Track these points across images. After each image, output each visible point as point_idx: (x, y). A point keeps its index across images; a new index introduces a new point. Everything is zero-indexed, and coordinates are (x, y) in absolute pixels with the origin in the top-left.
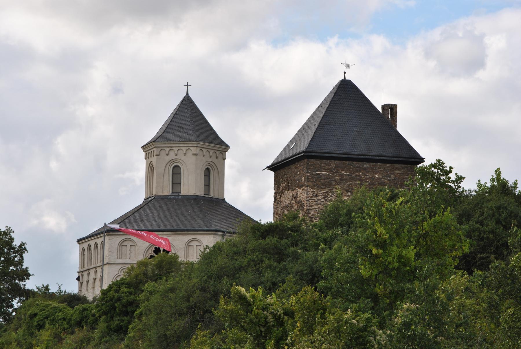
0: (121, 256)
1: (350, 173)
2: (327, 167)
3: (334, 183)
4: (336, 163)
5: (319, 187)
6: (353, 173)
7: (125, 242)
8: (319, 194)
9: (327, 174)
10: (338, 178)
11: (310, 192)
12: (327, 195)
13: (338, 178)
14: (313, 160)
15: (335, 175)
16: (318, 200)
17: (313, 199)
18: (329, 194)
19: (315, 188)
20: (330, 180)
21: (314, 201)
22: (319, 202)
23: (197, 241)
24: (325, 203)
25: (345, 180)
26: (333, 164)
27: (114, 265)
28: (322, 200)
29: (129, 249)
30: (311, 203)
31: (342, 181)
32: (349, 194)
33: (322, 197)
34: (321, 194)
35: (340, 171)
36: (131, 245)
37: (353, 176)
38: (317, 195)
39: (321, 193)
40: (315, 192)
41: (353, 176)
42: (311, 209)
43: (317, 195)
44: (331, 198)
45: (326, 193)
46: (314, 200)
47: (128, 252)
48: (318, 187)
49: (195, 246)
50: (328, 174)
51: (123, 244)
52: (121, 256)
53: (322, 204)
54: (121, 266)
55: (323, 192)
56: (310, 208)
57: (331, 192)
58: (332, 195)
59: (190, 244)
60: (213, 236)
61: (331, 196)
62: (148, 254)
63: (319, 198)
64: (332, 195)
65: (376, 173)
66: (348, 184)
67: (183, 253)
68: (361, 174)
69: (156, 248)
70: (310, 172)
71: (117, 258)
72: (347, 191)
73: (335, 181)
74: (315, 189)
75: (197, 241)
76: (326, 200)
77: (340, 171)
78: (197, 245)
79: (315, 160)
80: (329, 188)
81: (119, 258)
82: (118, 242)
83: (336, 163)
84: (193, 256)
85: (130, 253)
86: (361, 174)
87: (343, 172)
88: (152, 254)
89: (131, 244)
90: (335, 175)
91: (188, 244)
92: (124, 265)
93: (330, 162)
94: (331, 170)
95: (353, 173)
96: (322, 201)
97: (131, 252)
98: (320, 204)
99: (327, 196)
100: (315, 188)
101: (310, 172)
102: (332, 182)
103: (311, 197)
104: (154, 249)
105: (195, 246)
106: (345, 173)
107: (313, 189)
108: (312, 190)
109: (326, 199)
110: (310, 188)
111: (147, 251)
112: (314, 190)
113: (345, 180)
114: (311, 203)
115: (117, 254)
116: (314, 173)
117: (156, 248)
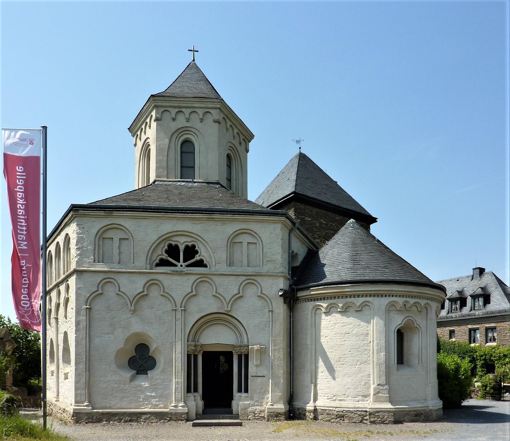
4: (317, 210)
9: (310, 219)
25: (323, 228)
26: (315, 210)
31: (321, 229)
35: (320, 219)
50: (311, 220)
51: (107, 235)
66: (325, 232)
67: (224, 256)
69: (170, 246)
73: (316, 227)
77: (320, 219)
80: (312, 233)
83: (317, 210)
86: (334, 224)
87: (322, 220)
88: (163, 257)
89: (122, 235)
94: (313, 217)
95: (328, 223)
97: (122, 251)
102: (314, 228)
104: (166, 247)
105: (245, 245)
111: (154, 250)
113: (323, 228)
115: (95, 254)
117: (170, 246)
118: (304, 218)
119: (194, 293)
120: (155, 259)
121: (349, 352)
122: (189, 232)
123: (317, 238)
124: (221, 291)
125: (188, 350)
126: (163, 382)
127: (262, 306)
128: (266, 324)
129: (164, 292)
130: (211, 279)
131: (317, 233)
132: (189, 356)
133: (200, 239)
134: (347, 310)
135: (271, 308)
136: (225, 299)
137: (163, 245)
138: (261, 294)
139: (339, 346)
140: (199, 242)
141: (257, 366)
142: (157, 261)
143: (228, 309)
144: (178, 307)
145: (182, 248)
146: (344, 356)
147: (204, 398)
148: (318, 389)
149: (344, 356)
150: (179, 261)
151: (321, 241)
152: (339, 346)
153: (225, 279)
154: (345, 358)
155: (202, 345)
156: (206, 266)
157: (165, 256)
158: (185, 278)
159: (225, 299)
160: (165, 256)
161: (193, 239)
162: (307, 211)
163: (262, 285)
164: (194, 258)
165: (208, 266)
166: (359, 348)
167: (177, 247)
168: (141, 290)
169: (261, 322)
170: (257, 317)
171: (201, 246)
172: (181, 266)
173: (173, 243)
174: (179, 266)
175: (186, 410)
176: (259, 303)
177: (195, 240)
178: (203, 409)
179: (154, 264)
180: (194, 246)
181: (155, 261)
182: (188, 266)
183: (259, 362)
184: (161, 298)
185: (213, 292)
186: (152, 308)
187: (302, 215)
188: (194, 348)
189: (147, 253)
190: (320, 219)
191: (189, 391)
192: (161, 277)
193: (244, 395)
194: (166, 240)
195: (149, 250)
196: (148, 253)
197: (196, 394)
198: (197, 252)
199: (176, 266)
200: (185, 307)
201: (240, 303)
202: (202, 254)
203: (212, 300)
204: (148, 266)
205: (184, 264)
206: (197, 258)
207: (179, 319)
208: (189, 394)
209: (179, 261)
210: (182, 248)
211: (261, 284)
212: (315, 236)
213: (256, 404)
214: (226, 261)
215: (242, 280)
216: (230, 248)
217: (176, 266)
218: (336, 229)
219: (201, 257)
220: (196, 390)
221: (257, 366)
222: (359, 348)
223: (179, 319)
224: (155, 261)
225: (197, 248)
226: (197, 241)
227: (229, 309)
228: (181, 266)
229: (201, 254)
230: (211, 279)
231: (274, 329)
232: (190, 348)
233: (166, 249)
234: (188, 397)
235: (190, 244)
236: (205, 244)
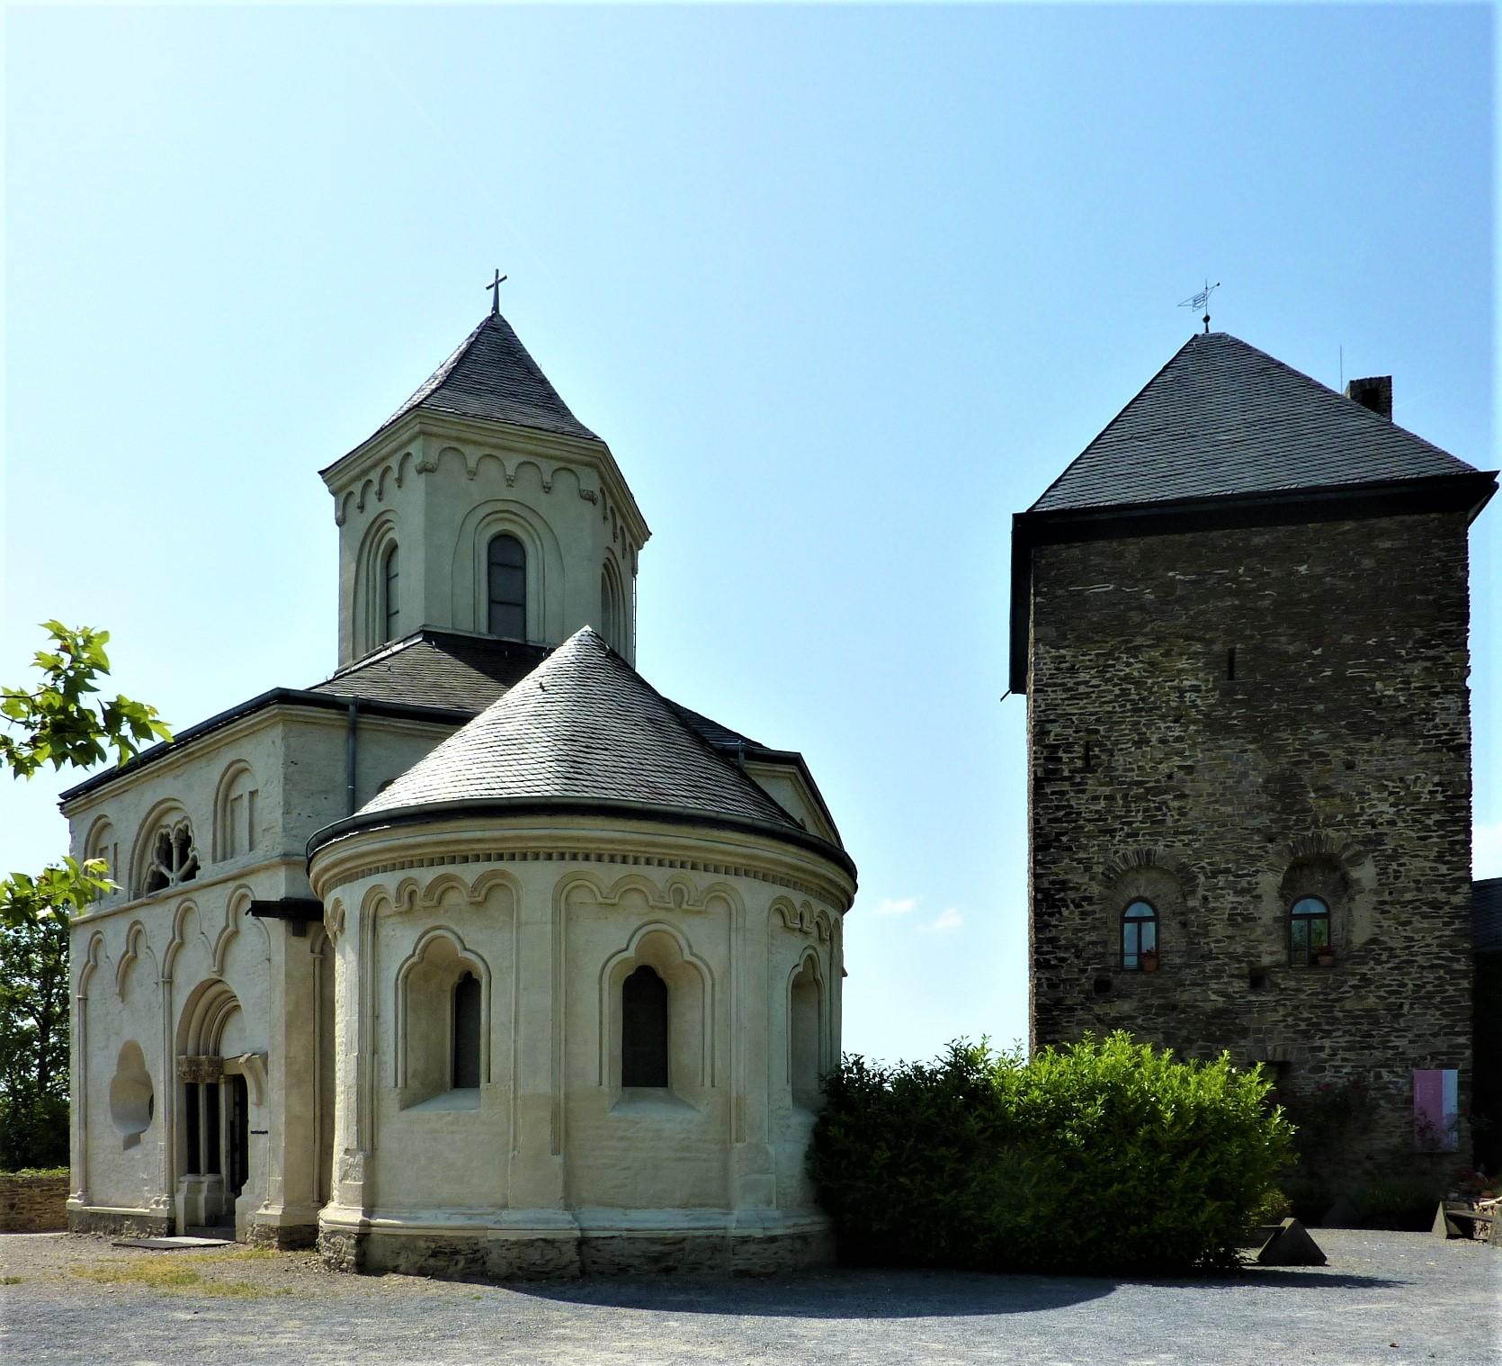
1: (1198, 575)
2: (1109, 564)
3: (1135, 617)
5: (1082, 640)
6: (1207, 573)
8: (1083, 661)
9: (1112, 587)
10: (1152, 597)
11: (1048, 661)
12: (1111, 662)
13: (1152, 597)
14: (1055, 547)
15: (1142, 587)
16: (1077, 684)
17: (1059, 681)
18: (1118, 659)
19: (1066, 643)
20: (1122, 607)
21: (1064, 691)
22: (1082, 689)
24: (1104, 691)
25: (1179, 601)
26: (1132, 549)
28: (1094, 682)
30: (1052, 696)
32: (1198, 647)
33: (1093, 672)
34: (1090, 661)
37: (1211, 582)
38: (1073, 666)
39: (1088, 658)
40: (1064, 657)
41: (1211, 582)
42: (1052, 717)
43: (1073, 666)
44: (1128, 670)
45: (1110, 655)
46: (1063, 684)
48: (1078, 638)
50: (1115, 589)
53: (1094, 695)
55: (1097, 655)
56: (1047, 716)
57: (1128, 651)
58: (1132, 660)
61: (1128, 665)
63: (1084, 676)
64: (1132, 660)
65: (1301, 562)
66: (1192, 613)
68: (1241, 571)
70: (1045, 589)
72: (1187, 638)
73: (1142, 608)
74: (1063, 648)
76: (1107, 681)
79: (1063, 546)
86: (1241, 571)
87: (1171, 574)
90: (1142, 587)
93: (1119, 546)
96: (1092, 686)
98: (1088, 695)
99: (1113, 666)
100: (1066, 643)
101: (1045, 589)
102: (1132, 614)
103: (1052, 676)
106: (1178, 577)
107: (1058, 648)
108: (1054, 652)
109: (1108, 675)
110: (1045, 645)
112: (1063, 652)
113: (1179, 601)
114: (1052, 696)
116: (1060, 592)
118: (1080, 593)
123: (1148, 646)
131: (1147, 630)
151: (1167, 654)
162: (1095, 560)
187: (1071, 583)
190: (1164, 570)
212: (1139, 641)
218: (1254, 585)
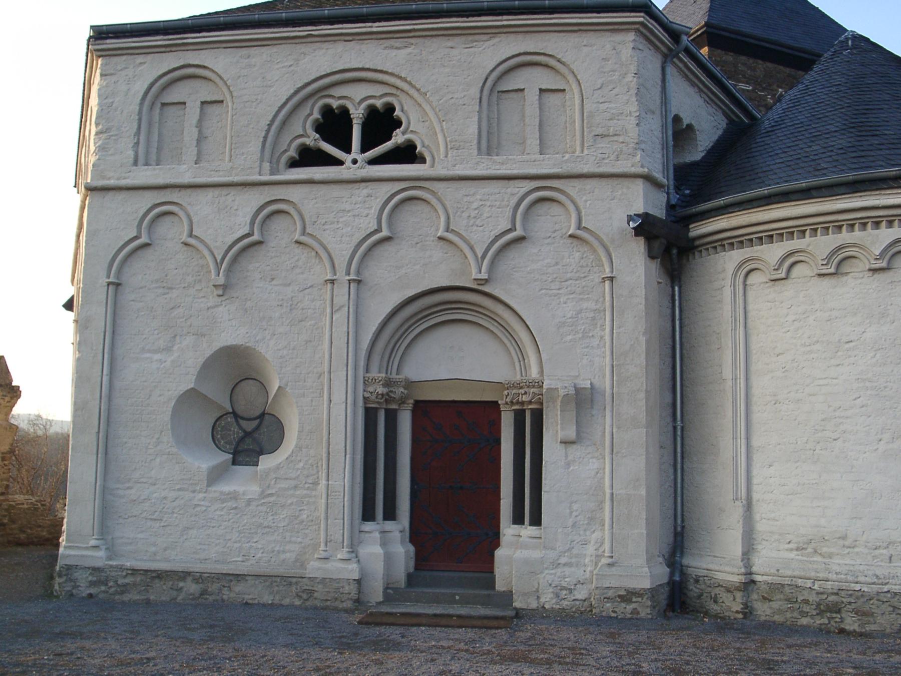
0: (153, 157)
7: (181, 84)
23: (546, 66)
27: (121, 196)
29: (194, 121)
36: (203, 103)
47: (190, 134)
49: (532, 96)
52: (153, 157)
54: (151, 198)
59: (504, 86)
60: (631, 36)
62: (286, 138)
67: (473, 129)
69: (327, 111)
71: (135, 163)
75: (546, 66)
78: (541, 90)
81: (147, 164)
82: (140, 87)
84: (524, 143)
85: (199, 141)
88: (309, 141)
91: (495, 84)
92: (168, 191)
104: (316, 115)
111: (284, 123)
117: (327, 111)
119: (385, 233)
120: (285, 147)
121: (855, 399)
122: (376, 71)
124: (459, 224)
125: (367, 395)
126: (296, 487)
127: (582, 267)
128: (593, 319)
129: (304, 232)
130: (433, 193)
132: (370, 415)
133: (405, 86)
134: (845, 268)
135: (607, 270)
136: (472, 248)
137: (308, 111)
138: (579, 229)
139: (821, 382)
140: (403, 97)
141: (566, 443)
142: (293, 153)
143: (479, 276)
144: (341, 276)
145: (357, 114)
146: (837, 414)
147: (416, 536)
148: (757, 517)
149: (837, 414)
150: (348, 150)
152: (821, 382)
153: (472, 191)
154: (841, 420)
155: (409, 384)
156: (423, 160)
157: (313, 139)
158: (364, 191)
159: (472, 248)
160: (313, 139)
161: (387, 90)
163: (581, 205)
164: (390, 139)
165: (428, 159)
166: (885, 387)
167: (345, 113)
168: (246, 230)
169: (580, 311)
170: (568, 299)
171: (408, 104)
172: (355, 162)
173: (335, 104)
174: (348, 163)
175: (352, 571)
176: (574, 256)
177: (394, 91)
178: (412, 570)
179: (284, 159)
180: (390, 108)
181: (286, 151)
182: (373, 162)
183: (571, 434)
184: (298, 250)
185: (437, 230)
186: (273, 279)
188: (381, 390)
189: (263, 134)
191: (368, 514)
192: (294, 194)
193: (528, 531)
194: (316, 97)
195: (270, 125)
196: (268, 131)
197: (390, 525)
198: (398, 124)
199: (340, 163)
200: (358, 272)
201: (516, 258)
202: (411, 129)
203: (437, 253)
204: (267, 165)
205: (361, 157)
206: (398, 138)
207: (343, 306)
208: (369, 526)
209: (348, 150)
210: (357, 114)
211: (578, 200)
213: (563, 560)
214: (475, 142)
215: (523, 191)
216: (489, 105)
217: (340, 163)
219: (407, 136)
220: (390, 514)
221: (566, 443)
222: (885, 387)
223: (343, 306)
224: (286, 151)
225: (397, 113)
226: (398, 93)
227: (484, 275)
228: (355, 162)
229: (408, 128)
230: (433, 193)
231: (618, 333)
232: (371, 389)
233: (317, 120)
234: (362, 535)
235: (379, 103)
236: (420, 99)
